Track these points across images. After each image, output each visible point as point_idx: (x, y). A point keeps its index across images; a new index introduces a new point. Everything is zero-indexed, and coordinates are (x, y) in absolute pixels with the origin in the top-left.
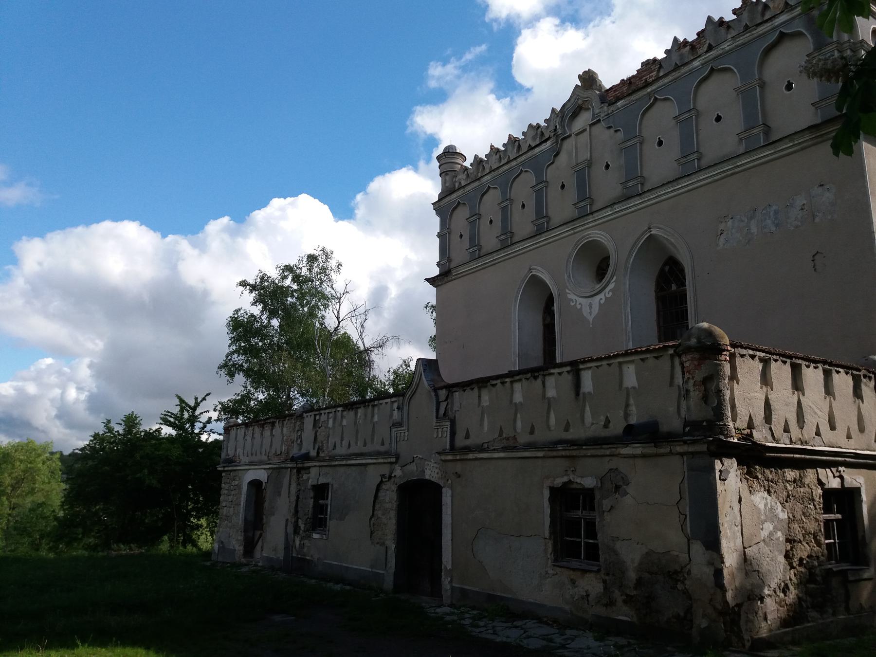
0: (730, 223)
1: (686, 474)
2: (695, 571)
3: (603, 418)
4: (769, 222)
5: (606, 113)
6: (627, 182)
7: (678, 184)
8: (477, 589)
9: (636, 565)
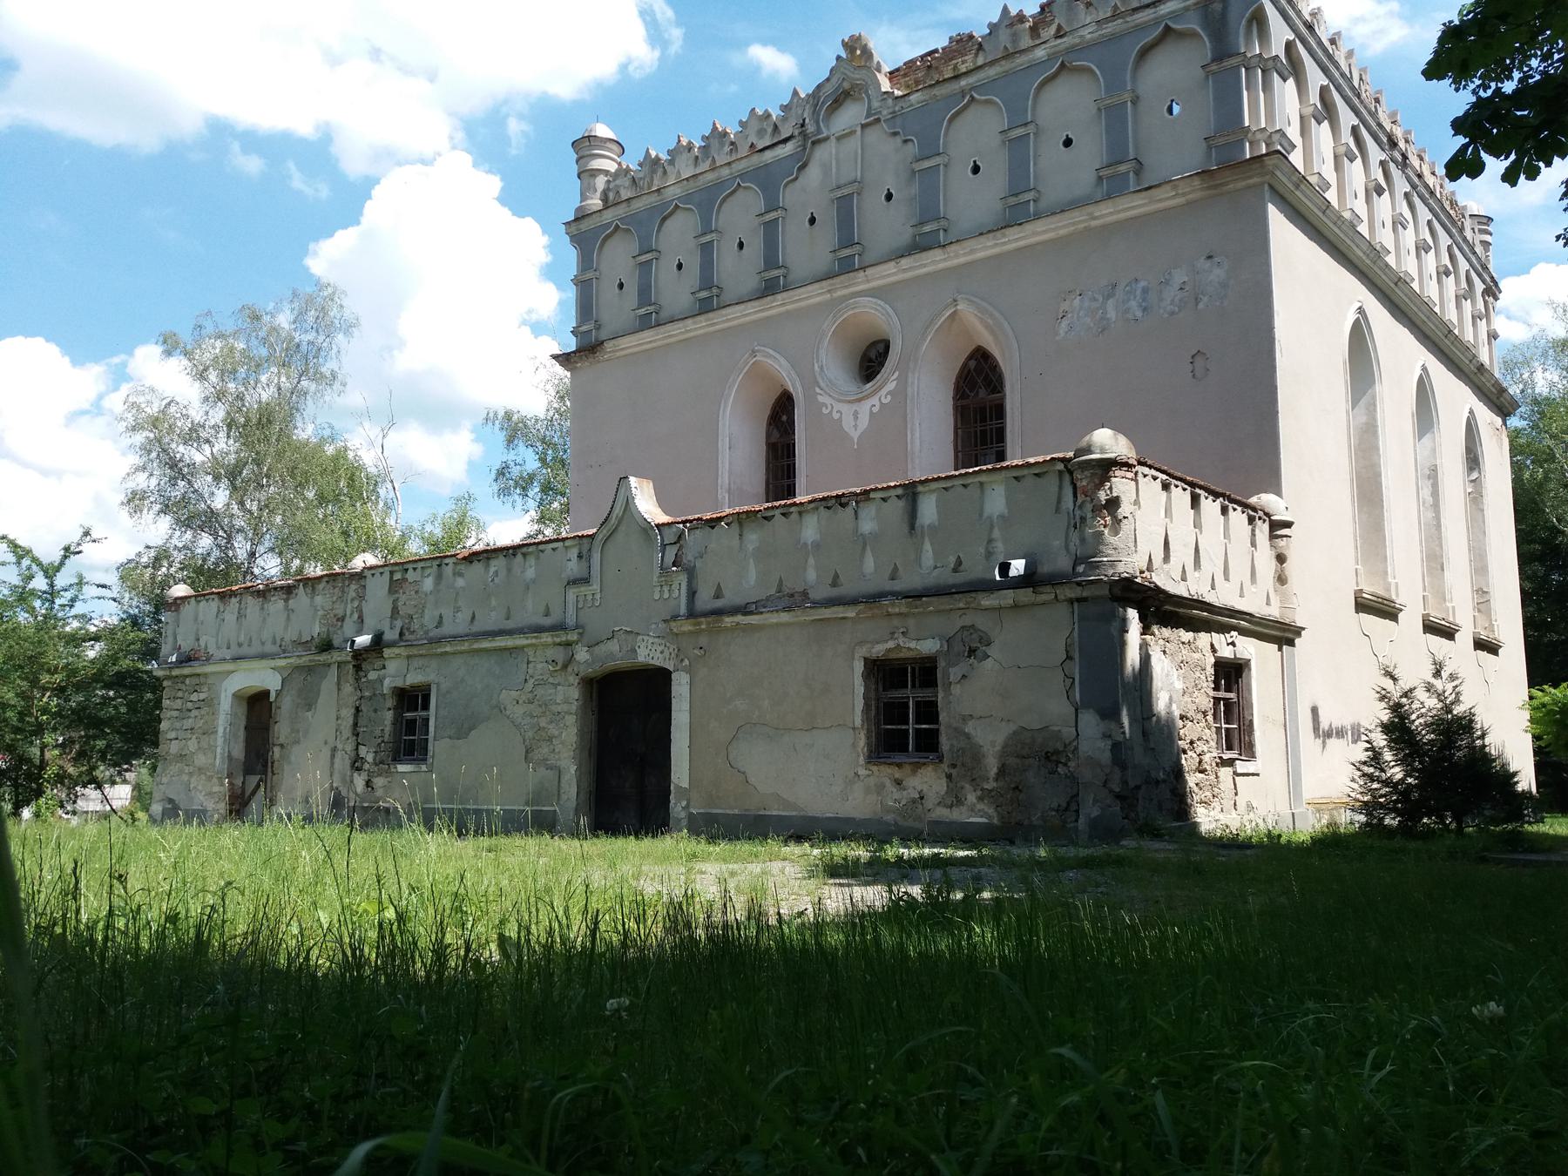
0: (1077, 301)
1: (1076, 626)
2: (1085, 748)
3: (952, 560)
4: (1133, 304)
5: (891, 110)
6: (922, 224)
7: (1004, 236)
8: (736, 812)
9: (998, 748)
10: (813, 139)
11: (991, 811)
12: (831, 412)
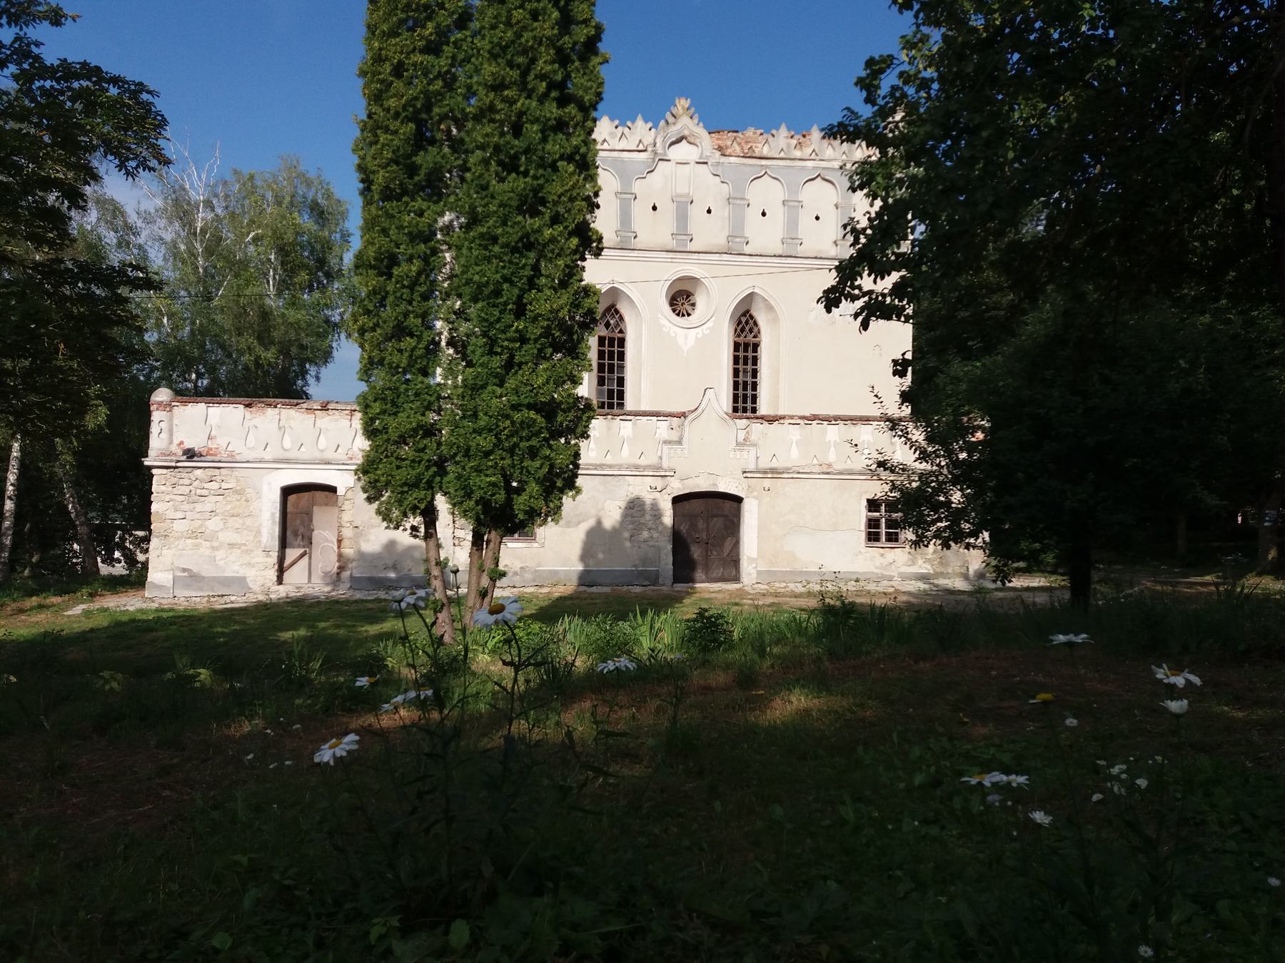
10: (661, 157)
11: (929, 567)
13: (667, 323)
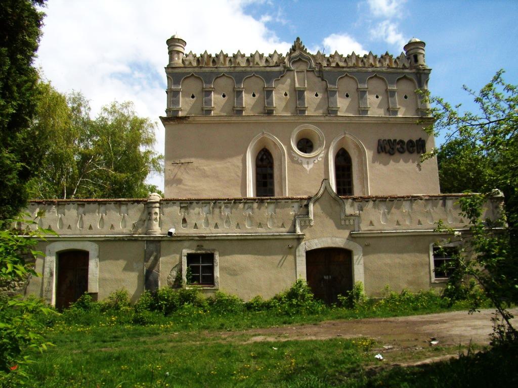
12: (297, 160)
13: (296, 156)
